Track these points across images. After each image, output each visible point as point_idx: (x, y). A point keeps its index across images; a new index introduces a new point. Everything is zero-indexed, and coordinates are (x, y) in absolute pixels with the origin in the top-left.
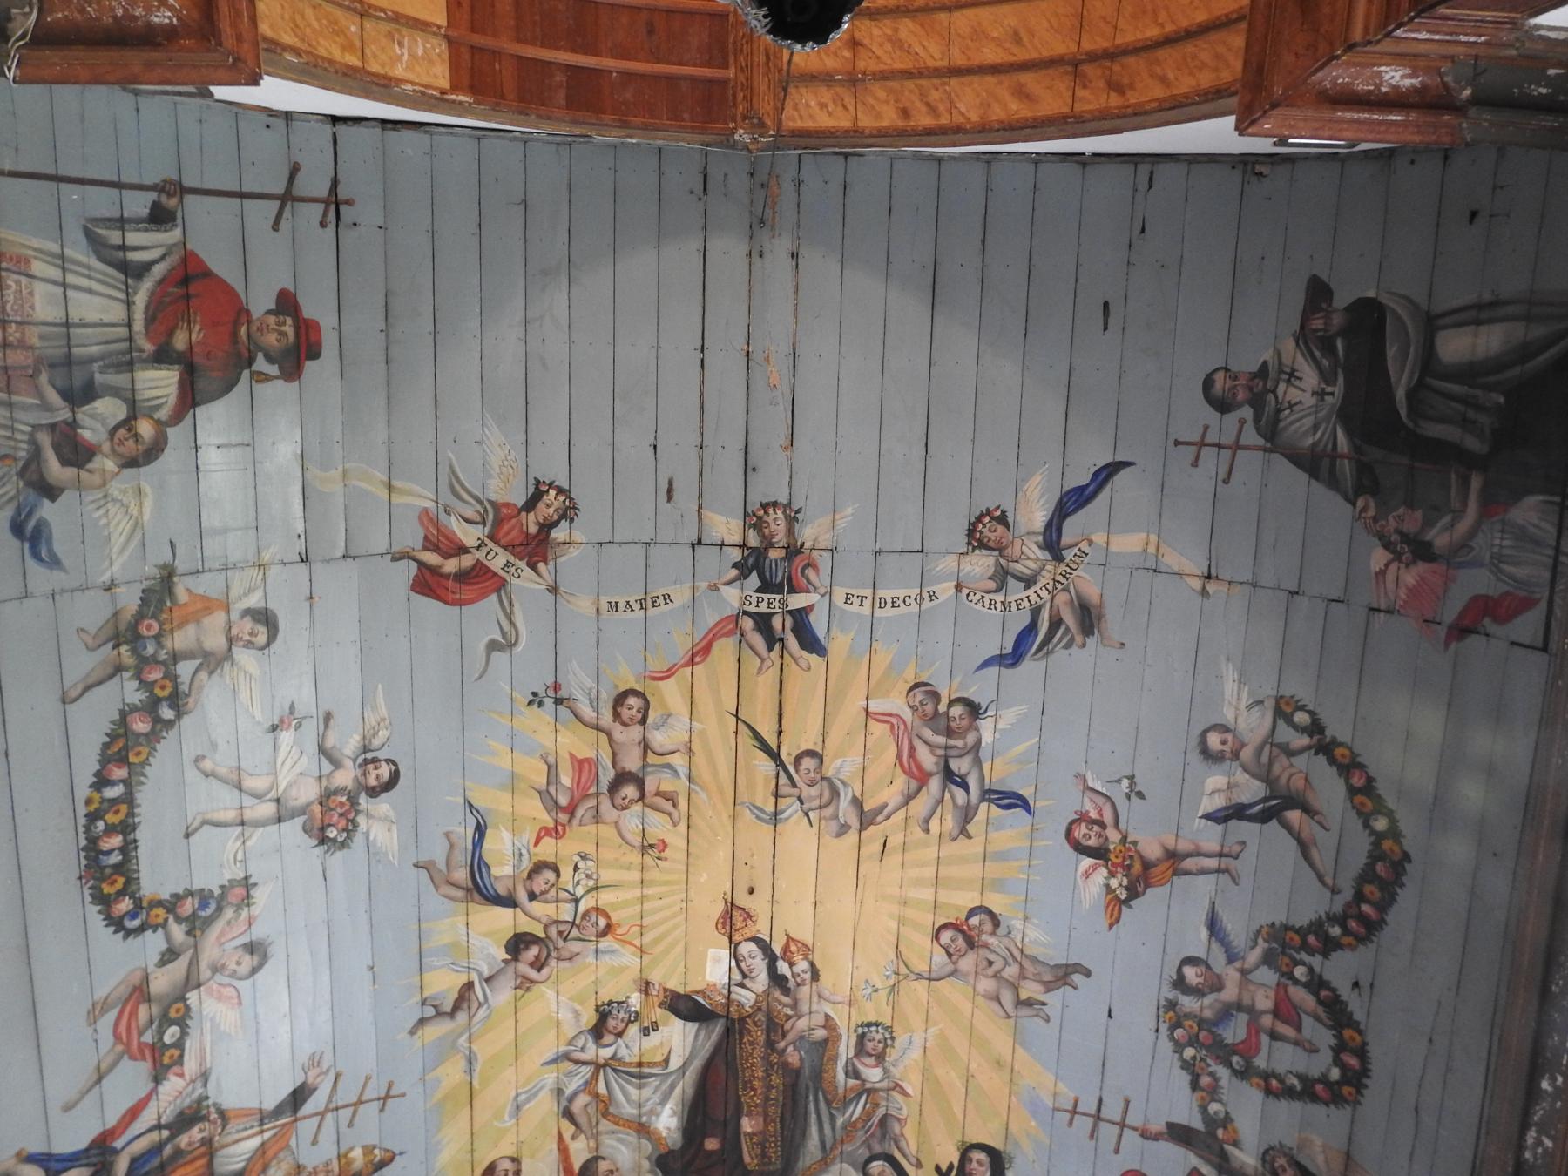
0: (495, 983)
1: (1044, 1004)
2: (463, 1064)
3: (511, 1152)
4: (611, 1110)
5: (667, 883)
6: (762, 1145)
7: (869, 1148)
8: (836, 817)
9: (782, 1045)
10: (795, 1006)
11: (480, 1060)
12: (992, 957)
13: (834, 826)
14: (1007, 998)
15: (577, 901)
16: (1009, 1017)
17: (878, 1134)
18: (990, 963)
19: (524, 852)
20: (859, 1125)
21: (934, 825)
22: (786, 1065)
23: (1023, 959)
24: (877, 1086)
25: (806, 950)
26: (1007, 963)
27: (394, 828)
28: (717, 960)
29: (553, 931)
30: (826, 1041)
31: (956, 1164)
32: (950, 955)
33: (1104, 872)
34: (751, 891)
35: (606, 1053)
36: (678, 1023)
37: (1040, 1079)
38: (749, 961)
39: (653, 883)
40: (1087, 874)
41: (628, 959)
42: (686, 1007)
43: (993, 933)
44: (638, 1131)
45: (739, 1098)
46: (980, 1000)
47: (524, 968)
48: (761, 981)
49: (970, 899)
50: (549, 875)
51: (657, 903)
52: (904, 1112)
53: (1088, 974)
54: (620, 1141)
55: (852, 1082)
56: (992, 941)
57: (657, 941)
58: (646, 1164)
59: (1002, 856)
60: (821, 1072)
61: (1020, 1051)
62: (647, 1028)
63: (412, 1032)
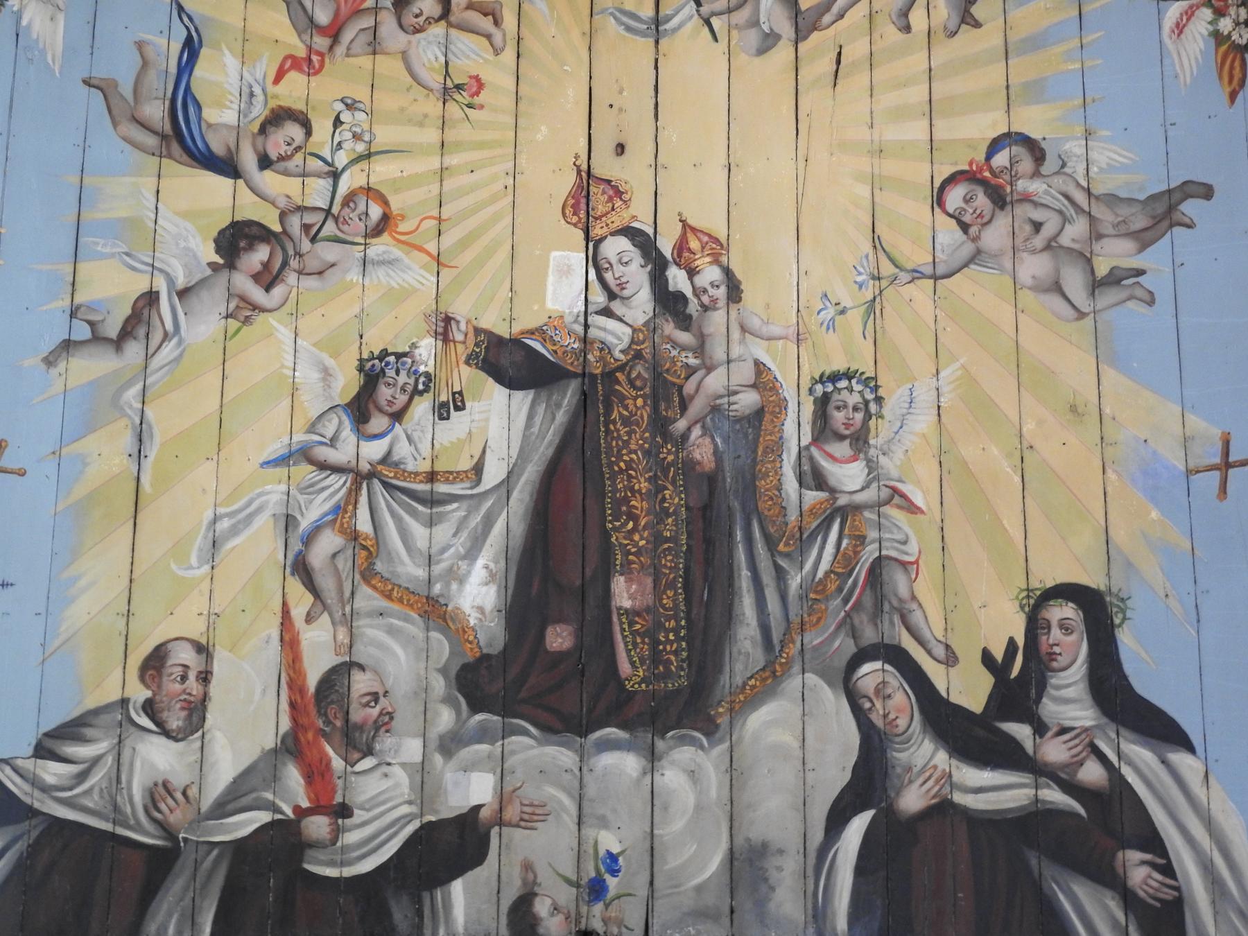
0: (193, 300)
1: (1140, 272)
2: (127, 440)
3: (196, 630)
4: (379, 566)
5: (481, 145)
6: (651, 633)
7: (854, 634)
8: (755, 23)
9: (681, 425)
10: (700, 349)
11: (158, 439)
12: (1038, 215)
13: (753, 37)
14: (1075, 282)
15: (335, 176)
16: (1081, 315)
17: (868, 601)
18: (1037, 226)
19: (257, 90)
20: (832, 587)
21: (918, 18)
22: (689, 466)
23: (1092, 202)
24: (860, 498)
25: (717, 248)
26: (1065, 220)
27: (61, 18)
28: (566, 271)
29: (295, 223)
30: (759, 413)
31: (1020, 642)
32: (965, 227)
33: (1207, 13)
34: (621, 149)
35: (373, 450)
36: (497, 394)
37: (1154, 421)
38: (619, 270)
39: (459, 146)
40: (1179, 28)
41: (416, 276)
42: (514, 362)
43: (1036, 174)
44: (425, 615)
45: (606, 535)
46: (1027, 297)
47: (243, 282)
48: (640, 305)
49: (991, 124)
50: (294, 131)
51: (467, 179)
52: (913, 547)
53: (1207, 192)
54: (391, 631)
55: (813, 497)
56: (1036, 187)
57: (464, 244)
58: (439, 685)
59: (1036, 43)
60: (754, 478)
61: (1109, 374)
62: (444, 405)
63: (50, 361)
